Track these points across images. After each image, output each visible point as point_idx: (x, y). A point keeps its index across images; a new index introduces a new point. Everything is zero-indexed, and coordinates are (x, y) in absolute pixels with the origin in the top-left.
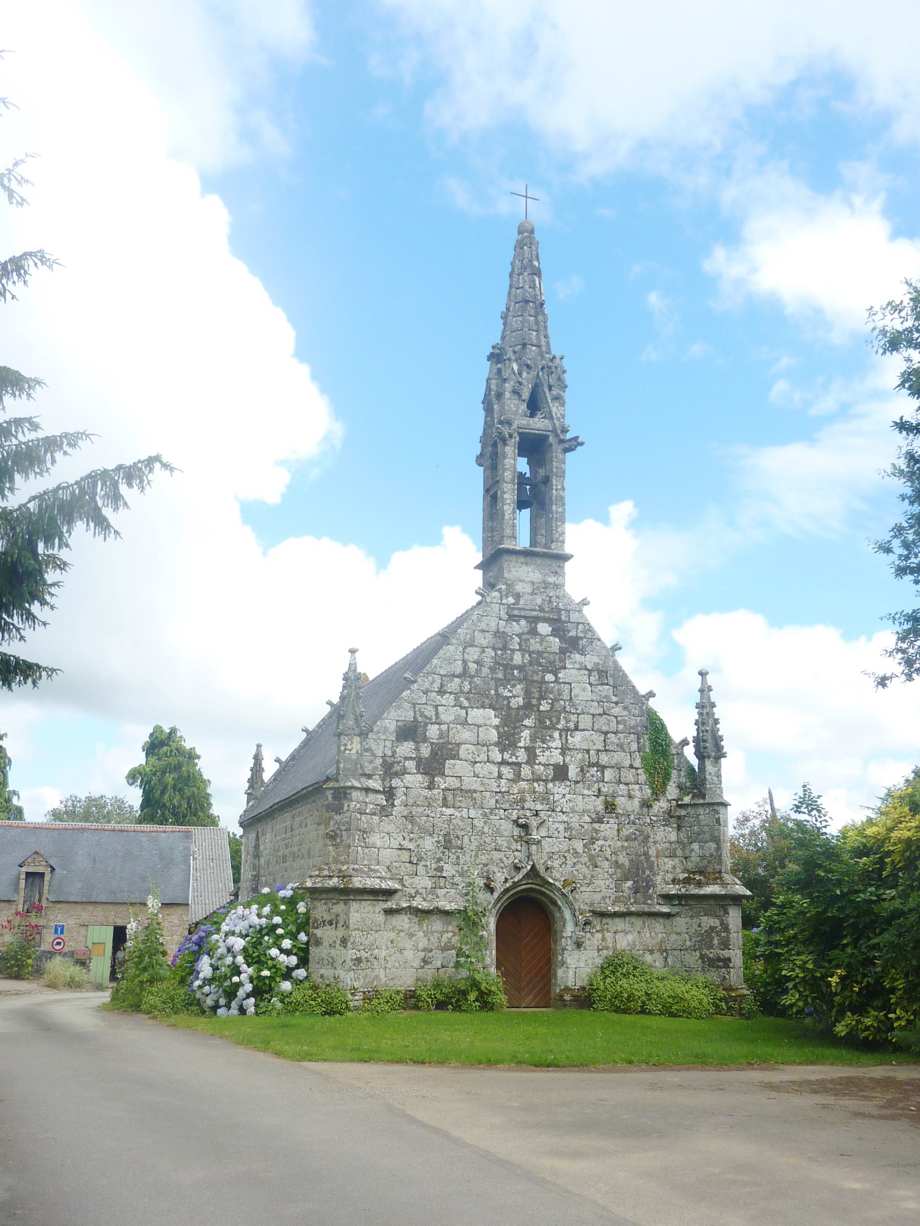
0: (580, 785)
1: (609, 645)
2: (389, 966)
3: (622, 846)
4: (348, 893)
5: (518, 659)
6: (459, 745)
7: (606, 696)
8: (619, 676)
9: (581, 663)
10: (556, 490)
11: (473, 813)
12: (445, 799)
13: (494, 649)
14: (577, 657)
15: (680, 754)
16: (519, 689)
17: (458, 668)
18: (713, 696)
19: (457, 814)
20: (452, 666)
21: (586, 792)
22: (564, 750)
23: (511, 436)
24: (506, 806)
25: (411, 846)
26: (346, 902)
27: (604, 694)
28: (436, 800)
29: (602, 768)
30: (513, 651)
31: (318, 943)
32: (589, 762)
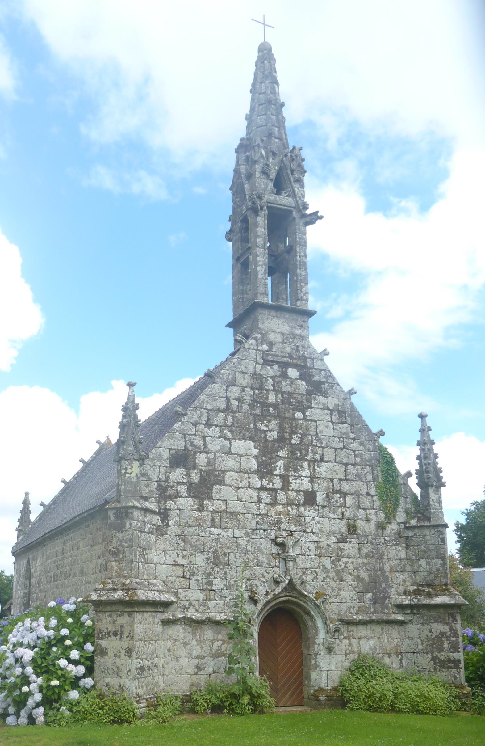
0: (326, 509)
1: (346, 389)
2: (166, 672)
3: (363, 563)
4: (132, 605)
5: (272, 398)
6: (224, 472)
7: (345, 433)
8: (355, 416)
9: (324, 404)
10: (300, 256)
11: (237, 533)
12: (213, 520)
13: (252, 388)
14: (321, 398)
15: (406, 484)
16: (273, 424)
17: (222, 404)
18: (432, 435)
19: (223, 533)
20: (217, 402)
21: (331, 515)
22: (313, 479)
23: (262, 208)
24: (265, 527)
25: (184, 562)
26: (130, 614)
27: (343, 431)
28: (205, 521)
29: (344, 495)
30: (268, 391)
31: (103, 652)
32: (333, 489)
